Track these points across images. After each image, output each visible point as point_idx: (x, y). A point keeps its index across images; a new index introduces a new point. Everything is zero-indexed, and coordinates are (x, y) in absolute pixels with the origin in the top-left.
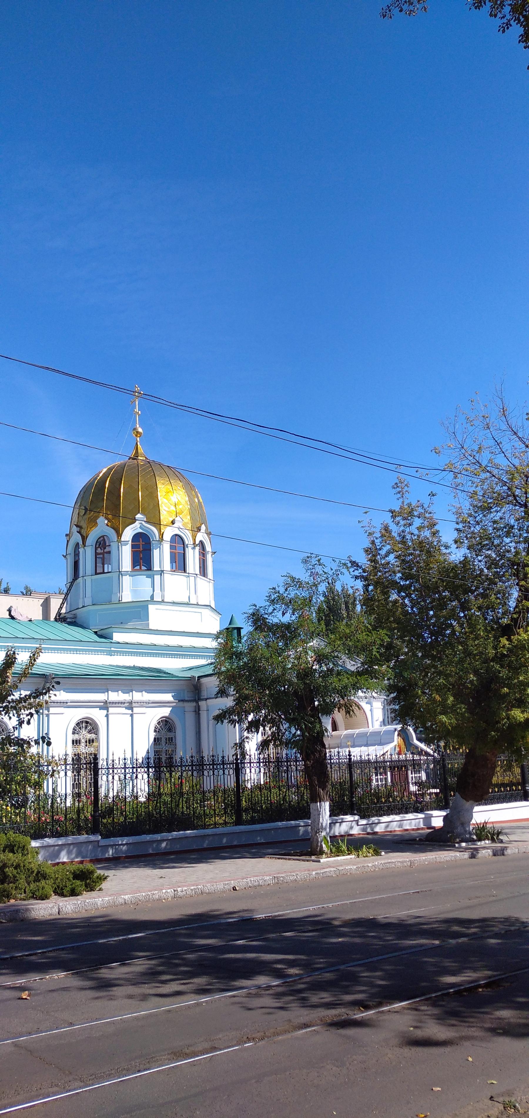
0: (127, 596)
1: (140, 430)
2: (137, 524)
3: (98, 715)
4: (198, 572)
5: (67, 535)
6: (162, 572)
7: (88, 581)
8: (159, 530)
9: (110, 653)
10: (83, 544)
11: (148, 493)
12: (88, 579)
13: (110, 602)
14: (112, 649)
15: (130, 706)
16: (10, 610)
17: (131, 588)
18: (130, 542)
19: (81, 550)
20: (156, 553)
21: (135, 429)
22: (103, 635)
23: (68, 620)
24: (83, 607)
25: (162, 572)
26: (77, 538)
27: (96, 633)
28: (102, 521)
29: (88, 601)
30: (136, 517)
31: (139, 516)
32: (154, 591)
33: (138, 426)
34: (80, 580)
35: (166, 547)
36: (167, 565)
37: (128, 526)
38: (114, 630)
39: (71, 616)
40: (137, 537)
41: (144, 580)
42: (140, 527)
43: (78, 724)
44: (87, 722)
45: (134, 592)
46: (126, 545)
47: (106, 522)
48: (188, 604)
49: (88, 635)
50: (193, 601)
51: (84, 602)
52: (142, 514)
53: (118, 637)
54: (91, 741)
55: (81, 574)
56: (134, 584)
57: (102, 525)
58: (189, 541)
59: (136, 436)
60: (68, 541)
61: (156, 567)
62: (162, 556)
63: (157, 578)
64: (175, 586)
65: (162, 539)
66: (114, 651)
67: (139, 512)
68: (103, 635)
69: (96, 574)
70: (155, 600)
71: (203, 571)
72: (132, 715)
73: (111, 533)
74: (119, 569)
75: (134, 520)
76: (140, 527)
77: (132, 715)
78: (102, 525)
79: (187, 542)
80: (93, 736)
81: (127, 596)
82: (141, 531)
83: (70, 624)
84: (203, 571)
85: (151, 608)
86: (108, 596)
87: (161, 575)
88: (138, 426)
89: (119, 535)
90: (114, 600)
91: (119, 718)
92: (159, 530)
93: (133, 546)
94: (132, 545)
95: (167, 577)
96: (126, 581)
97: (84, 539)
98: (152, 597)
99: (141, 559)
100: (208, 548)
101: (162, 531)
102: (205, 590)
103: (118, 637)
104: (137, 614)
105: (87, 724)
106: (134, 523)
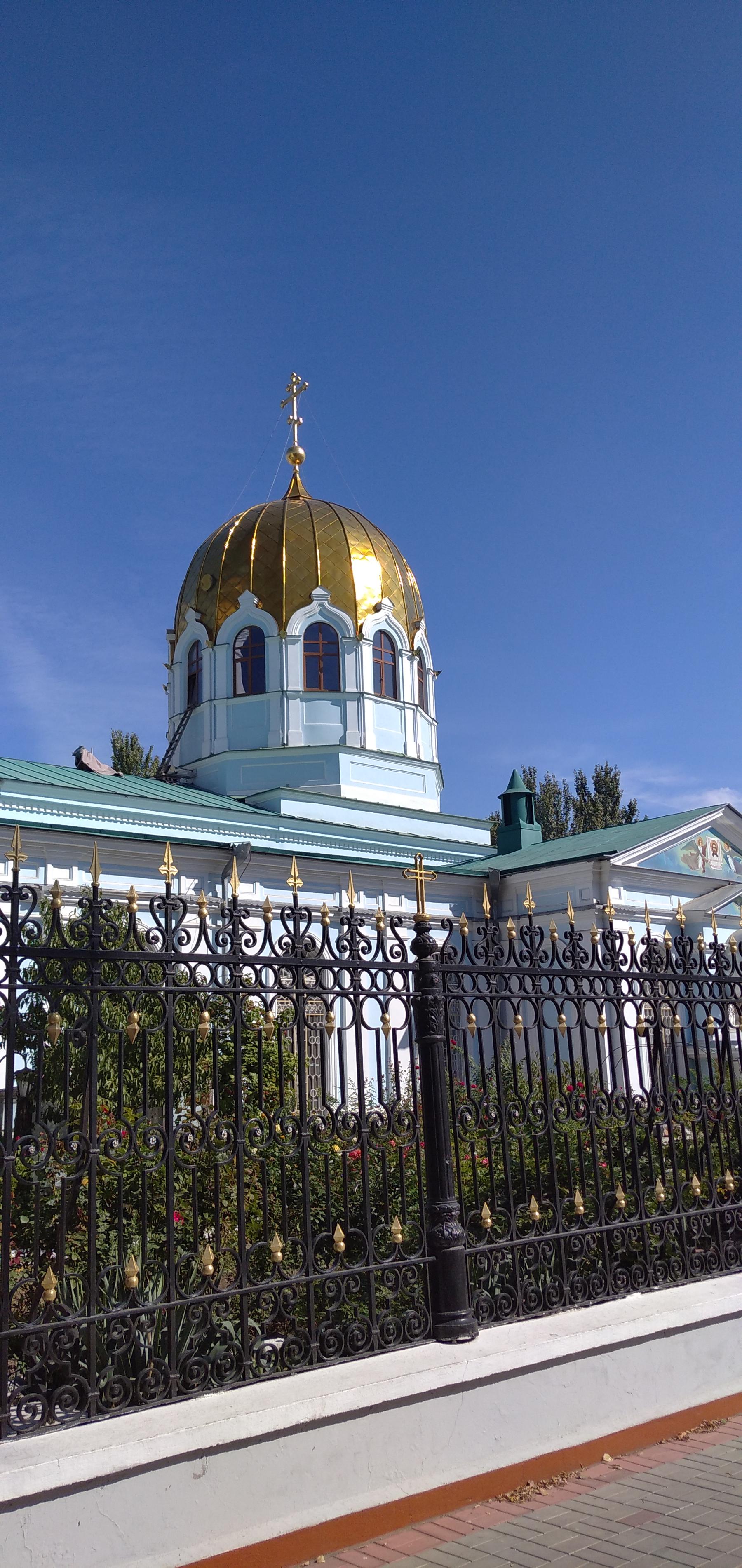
0: (297, 736)
1: (301, 451)
2: (315, 606)
5: (169, 632)
6: (360, 696)
7: (222, 710)
8: (355, 618)
10: (211, 640)
11: (331, 551)
12: (221, 706)
13: (265, 748)
14: (282, 829)
16: (78, 755)
17: (302, 723)
18: (302, 639)
19: (206, 654)
20: (349, 660)
21: (291, 449)
23: (182, 780)
24: (212, 755)
25: (360, 696)
26: (195, 630)
28: (249, 600)
29: (220, 745)
30: (314, 592)
31: (318, 591)
32: (345, 729)
33: (296, 444)
34: (204, 708)
35: (367, 652)
36: (368, 686)
37: (298, 608)
39: (186, 773)
40: (314, 631)
41: (326, 708)
42: (320, 613)
45: (310, 730)
47: (256, 600)
48: (403, 758)
50: (412, 753)
51: (212, 746)
52: (324, 587)
55: (206, 693)
56: (311, 716)
57: (249, 608)
59: (294, 462)
60: (173, 644)
61: (350, 688)
62: (361, 668)
63: (351, 706)
64: (381, 724)
66: (284, 834)
67: (317, 585)
69: (236, 695)
70: (348, 745)
71: (423, 703)
73: (266, 622)
74: (282, 687)
75: (309, 600)
76: (320, 613)
78: (249, 608)
81: (297, 736)
82: (321, 619)
83: (186, 785)
84: (423, 703)
85: (344, 759)
87: (359, 701)
88: (296, 444)
89: (282, 626)
90: (273, 742)
93: (306, 647)
94: (305, 644)
95: (369, 705)
96: (296, 710)
98: (343, 739)
99: (321, 670)
101: (360, 623)
102: (424, 740)
103: (288, 807)
104: (318, 771)
106: (310, 603)
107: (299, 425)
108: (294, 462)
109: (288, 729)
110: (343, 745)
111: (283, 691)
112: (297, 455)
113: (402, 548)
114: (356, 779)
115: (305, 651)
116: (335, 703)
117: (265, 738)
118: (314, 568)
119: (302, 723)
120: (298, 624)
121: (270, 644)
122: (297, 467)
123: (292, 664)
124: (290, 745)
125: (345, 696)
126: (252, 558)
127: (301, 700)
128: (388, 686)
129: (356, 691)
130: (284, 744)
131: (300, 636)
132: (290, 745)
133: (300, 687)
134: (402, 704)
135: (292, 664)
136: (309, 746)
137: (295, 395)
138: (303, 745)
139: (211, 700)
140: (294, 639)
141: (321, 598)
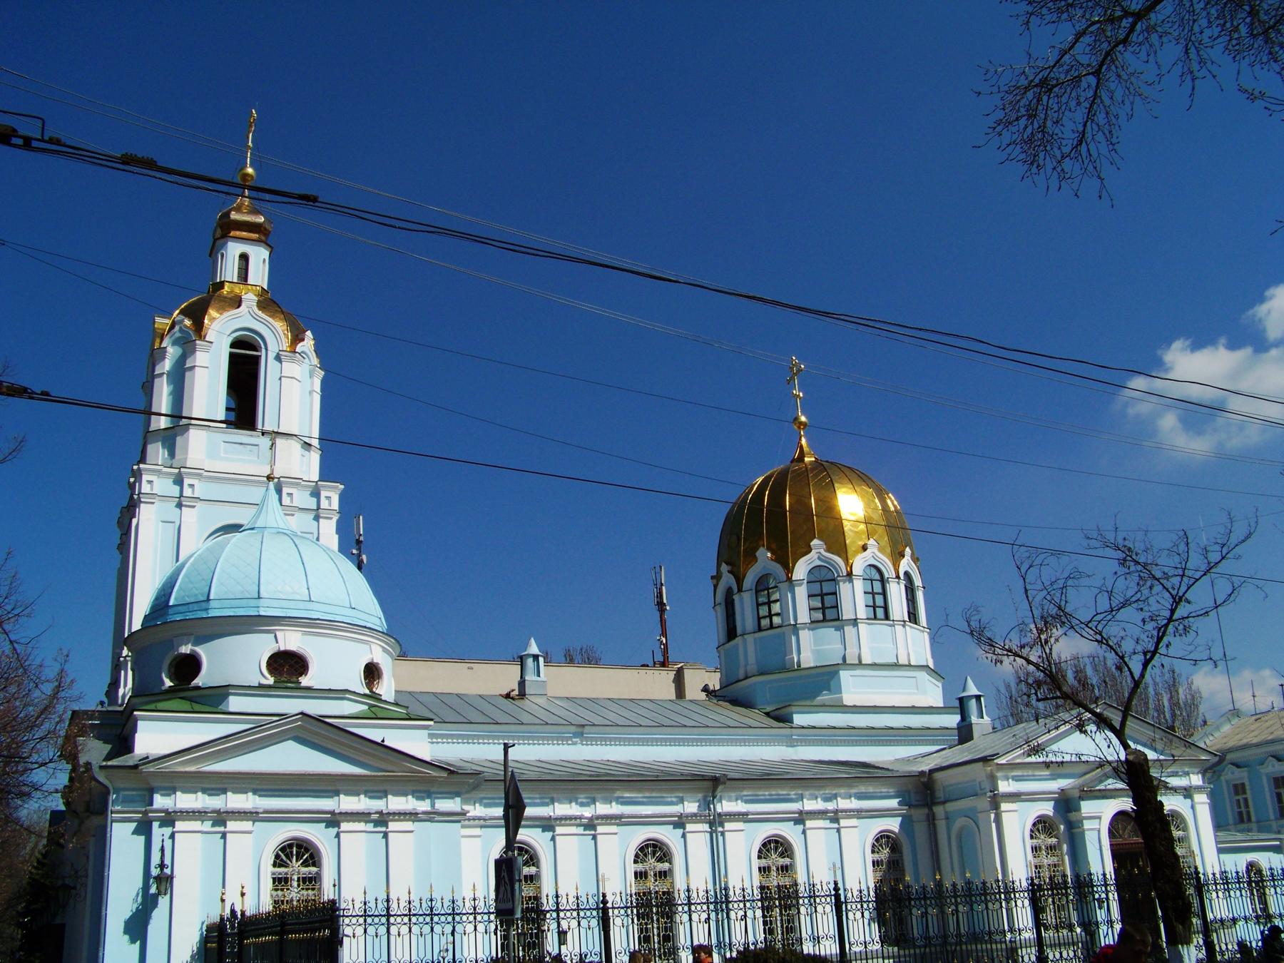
1: (803, 419)
3: (789, 832)
4: (906, 618)
5: (712, 577)
6: (855, 622)
8: (846, 560)
9: (791, 743)
15: (835, 816)
17: (811, 648)
19: (736, 597)
21: (796, 419)
22: (781, 717)
26: (728, 580)
27: (768, 714)
28: (764, 555)
31: (815, 542)
35: (859, 585)
36: (862, 613)
38: (794, 709)
41: (829, 633)
43: (764, 845)
44: (777, 842)
45: (817, 653)
47: (769, 555)
48: (896, 666)
49: (754, 718)
50: (903, 661)
52: (820, 539)
53: (799, 719)
54: (785, 869)
58: (889, 572)
60: (715, 587)
61: (847, 614)
62: (854, 598)
65: (850, 574)
68: (781, 717)
69: (760, 629)
71: (913, 617)
72: (838, 830)
73: (778, 569)
75: (809, 550)
77: (838, 830)
79: (886, 575)
80: (787, 861)
84: (913, 617)
85: (844, 674)
86: (778, 663)
89: (789, 570)
91: (819, 832)
92: (846, 560)
97: (739, 581)
98: (844, 658)
100: (918, 582)
102: (915, 644)
105: (776, 846)
110: (844, 663)
112: (801, 423)
114: (853, 688)
119: (811, 648)
120: (801, 570)
123: (801, 604)
124: (803, 666)
128: (880, 610)
141: (818, 547)
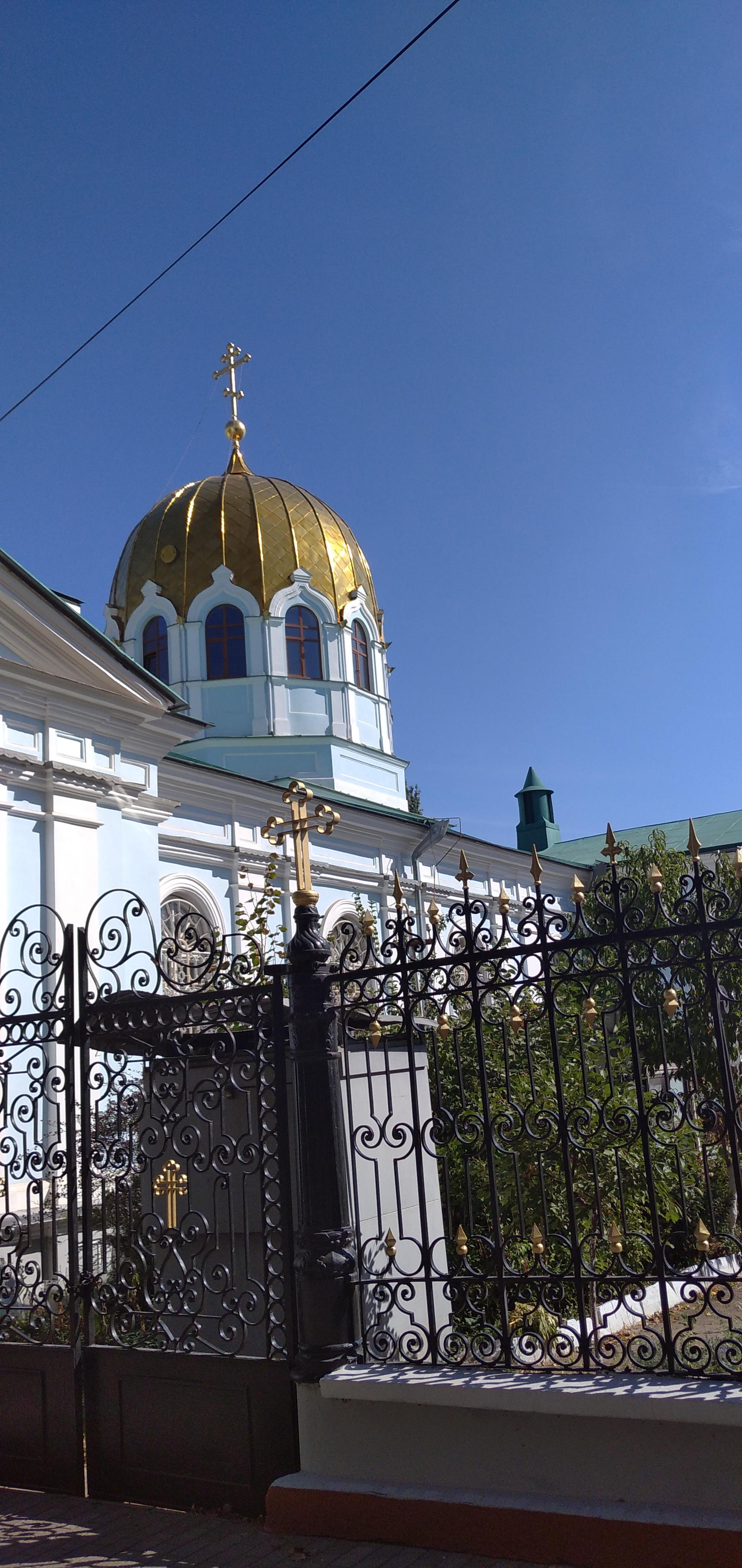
1: (242, 426)
18: (284, 621)
20: (332, 647)
21: (231, 423)
28: (223, 575)
30: (295, 573)
32: (331, 721)
33: (236, 418)
37: (279, 588)
41: (311, 697)
42: (301, 595)
45: (296, 719)
46: (277, 625)
56: (296, 704)
62: (340, 657)
63: (336, 695)
73: (243, 599)
76: (301, 595)
82: (301, 602)
85: (336, 751)
87: (343, 691)
88: (236, 418)
90: (258, 729)
95: (351, 694)
96: (281, 695)
98: (330, 729)
107: (240, 399)
108: (234, 437)
109: (274, 717)
111: (267, 676)
112: (238, 430)
113: (358, 536)
115: (287, 634)
116: (320, 692)
117: (252, 725)
118: (291, 548)
119: (290, 711)
121: (251, 626)
122: (237, 442)
123: (276, 648)
124: (277, 734)
125: (330, 685)
126: (223, 530)
127: (286, 687)
129: (342, 680)
130: (272, 733)
131: (282, 618)
132: (277, 734)
133: (284, 673)
134: (376, 698)
135: (276, 648)
136: (300, 736)
137: (233, 366)
138: (289, 734)
139: (182, 682)
140: (276, 622)
141: (302, 579)
